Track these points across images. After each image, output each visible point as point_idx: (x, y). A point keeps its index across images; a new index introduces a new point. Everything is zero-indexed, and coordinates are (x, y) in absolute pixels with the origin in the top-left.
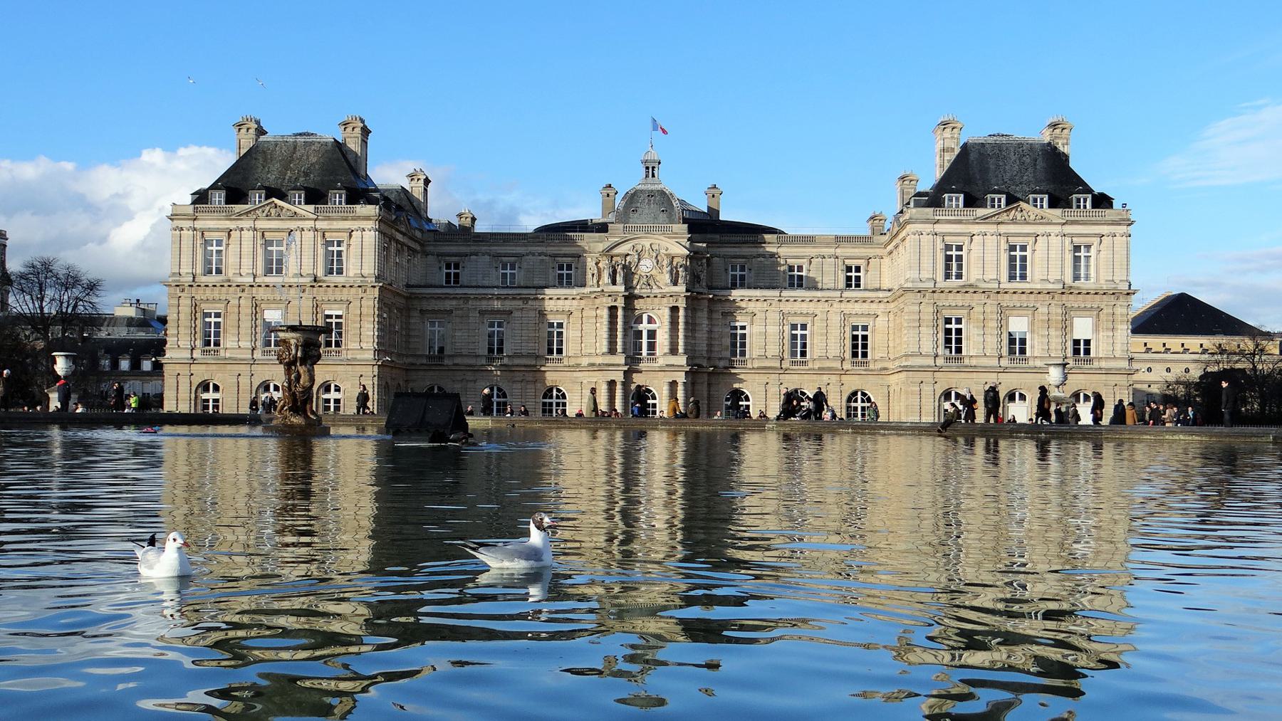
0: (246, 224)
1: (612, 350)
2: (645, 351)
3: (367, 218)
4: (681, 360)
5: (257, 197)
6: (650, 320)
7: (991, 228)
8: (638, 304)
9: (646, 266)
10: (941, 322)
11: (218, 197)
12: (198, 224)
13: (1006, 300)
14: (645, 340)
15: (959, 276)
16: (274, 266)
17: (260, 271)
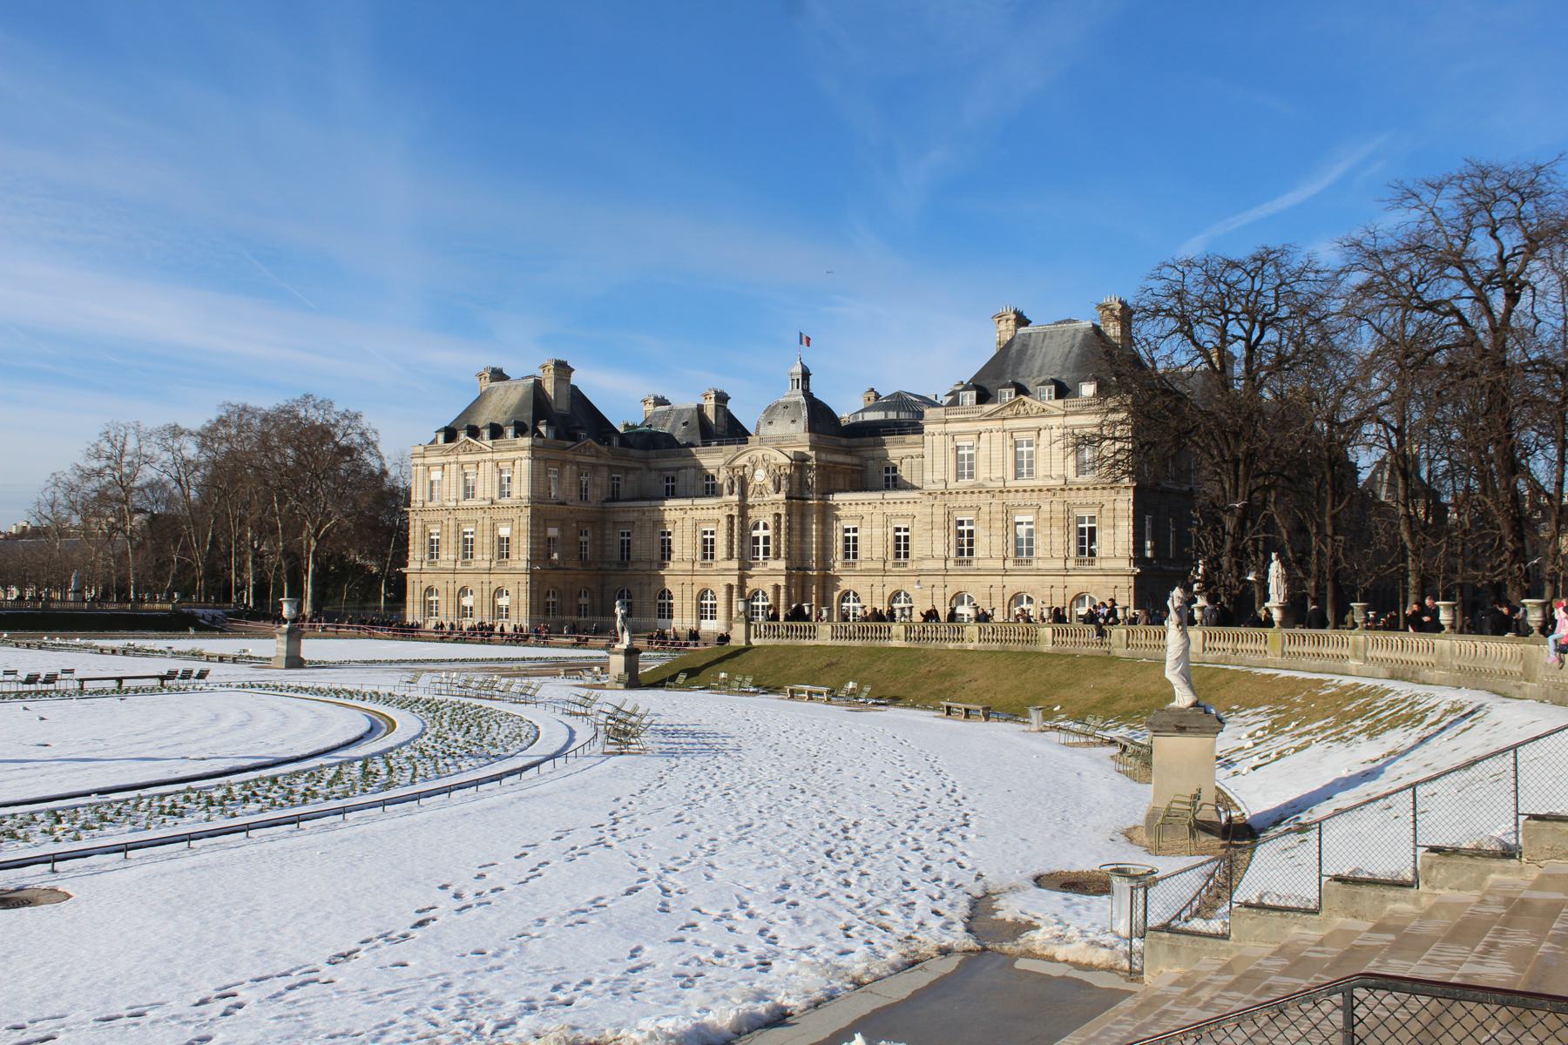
0: (452, 458)
1: (730, 557)
2: (761, 556)
3: (522, 449)
4: (781, 565)
5: (463, 436)
6: (766, 527)
7: (997, 425)
8: (750, 512)
9: (760, 476)
10: (952, 525)
11: (441, 437)
12: (427, 461)
13: (1011, 499)
14: (761, 546)
15: (971, 476)
16: (469, 492)
17: (461, 497)
